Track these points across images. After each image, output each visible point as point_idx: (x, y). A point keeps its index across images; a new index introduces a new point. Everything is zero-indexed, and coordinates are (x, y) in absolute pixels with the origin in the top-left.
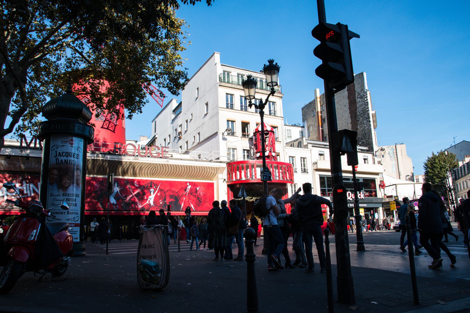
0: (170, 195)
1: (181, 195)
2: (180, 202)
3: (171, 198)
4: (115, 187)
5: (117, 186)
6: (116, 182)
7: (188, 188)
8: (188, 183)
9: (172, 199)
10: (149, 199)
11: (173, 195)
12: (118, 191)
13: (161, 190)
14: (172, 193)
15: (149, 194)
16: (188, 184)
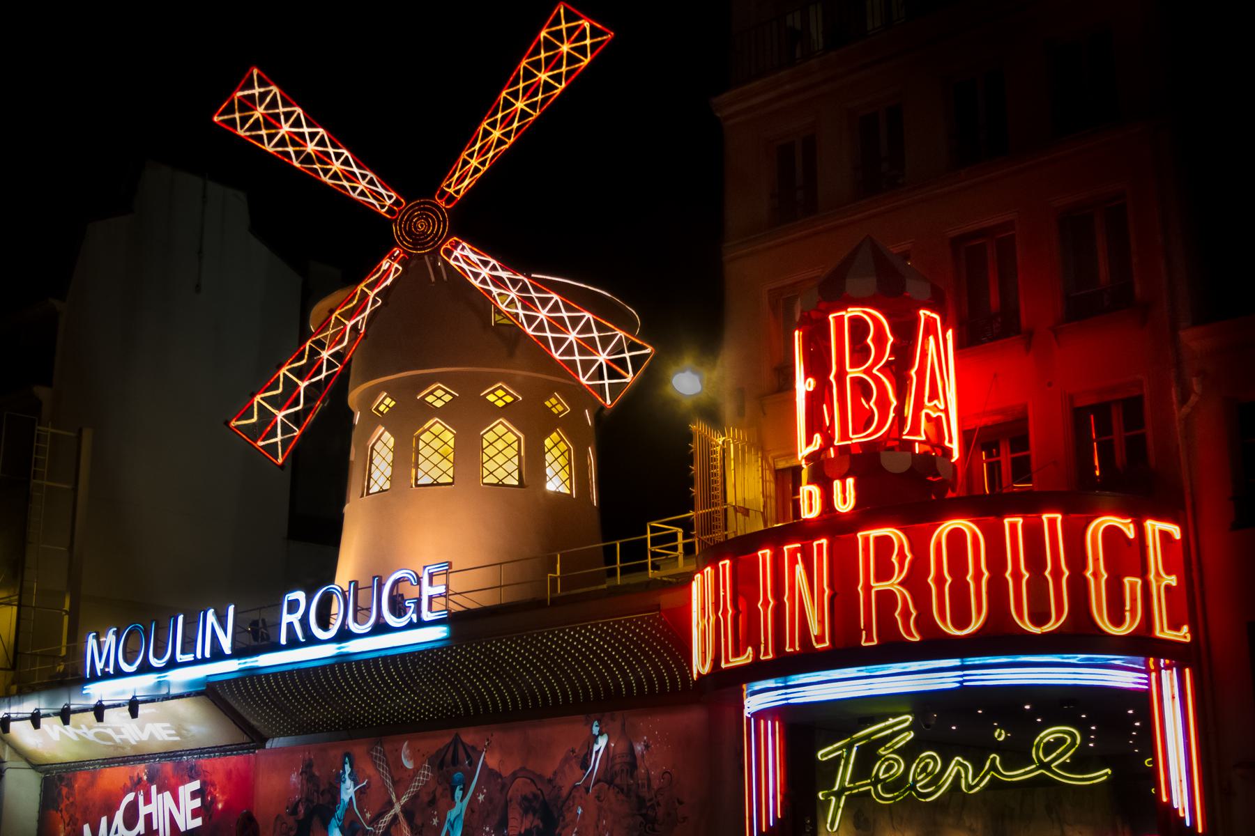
0: (525, 798)
1: (565, 792)
2: (563, 833)
3: (526, 812)
4: (344, 782)
5: (349, 775)
6: (347, 759)
7: (596, 748)
8: (596, 723)
9: (530, 817)
10: (446, 826)
11: (535, 796)
12: (351, 799)
13: (491, 770)
14: (534, 789)
15: (449, 798)
16: (596, 730)
